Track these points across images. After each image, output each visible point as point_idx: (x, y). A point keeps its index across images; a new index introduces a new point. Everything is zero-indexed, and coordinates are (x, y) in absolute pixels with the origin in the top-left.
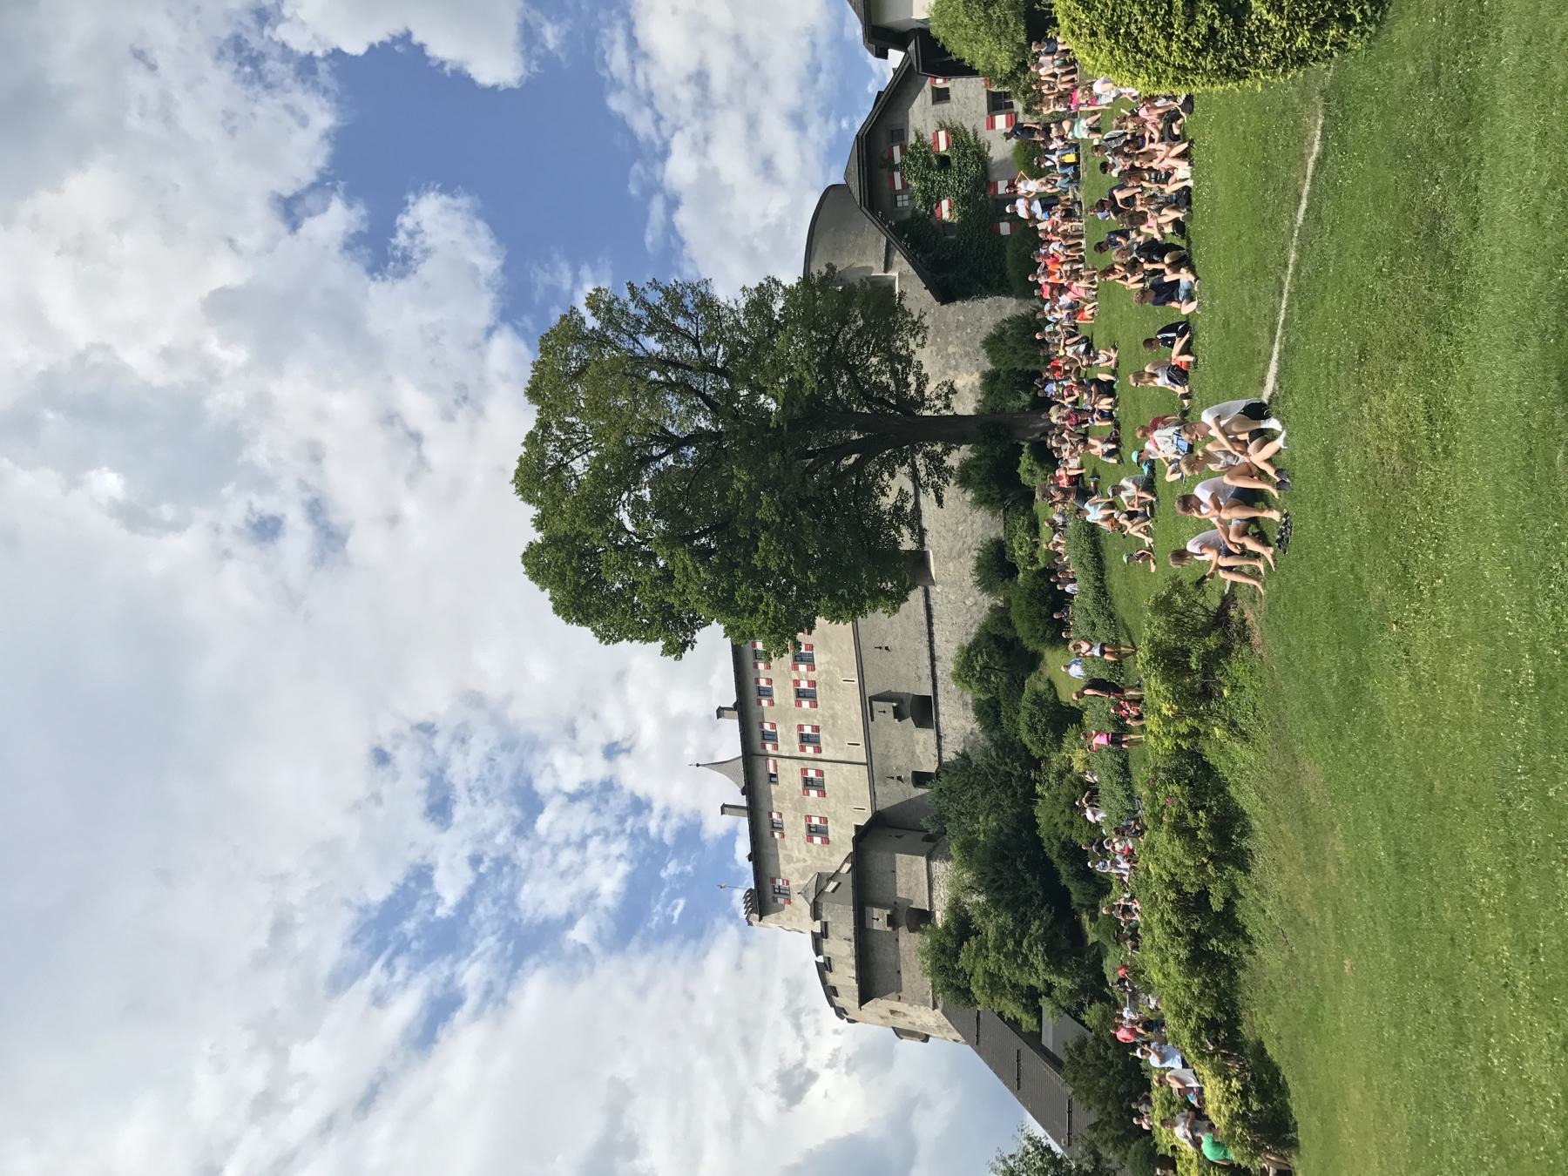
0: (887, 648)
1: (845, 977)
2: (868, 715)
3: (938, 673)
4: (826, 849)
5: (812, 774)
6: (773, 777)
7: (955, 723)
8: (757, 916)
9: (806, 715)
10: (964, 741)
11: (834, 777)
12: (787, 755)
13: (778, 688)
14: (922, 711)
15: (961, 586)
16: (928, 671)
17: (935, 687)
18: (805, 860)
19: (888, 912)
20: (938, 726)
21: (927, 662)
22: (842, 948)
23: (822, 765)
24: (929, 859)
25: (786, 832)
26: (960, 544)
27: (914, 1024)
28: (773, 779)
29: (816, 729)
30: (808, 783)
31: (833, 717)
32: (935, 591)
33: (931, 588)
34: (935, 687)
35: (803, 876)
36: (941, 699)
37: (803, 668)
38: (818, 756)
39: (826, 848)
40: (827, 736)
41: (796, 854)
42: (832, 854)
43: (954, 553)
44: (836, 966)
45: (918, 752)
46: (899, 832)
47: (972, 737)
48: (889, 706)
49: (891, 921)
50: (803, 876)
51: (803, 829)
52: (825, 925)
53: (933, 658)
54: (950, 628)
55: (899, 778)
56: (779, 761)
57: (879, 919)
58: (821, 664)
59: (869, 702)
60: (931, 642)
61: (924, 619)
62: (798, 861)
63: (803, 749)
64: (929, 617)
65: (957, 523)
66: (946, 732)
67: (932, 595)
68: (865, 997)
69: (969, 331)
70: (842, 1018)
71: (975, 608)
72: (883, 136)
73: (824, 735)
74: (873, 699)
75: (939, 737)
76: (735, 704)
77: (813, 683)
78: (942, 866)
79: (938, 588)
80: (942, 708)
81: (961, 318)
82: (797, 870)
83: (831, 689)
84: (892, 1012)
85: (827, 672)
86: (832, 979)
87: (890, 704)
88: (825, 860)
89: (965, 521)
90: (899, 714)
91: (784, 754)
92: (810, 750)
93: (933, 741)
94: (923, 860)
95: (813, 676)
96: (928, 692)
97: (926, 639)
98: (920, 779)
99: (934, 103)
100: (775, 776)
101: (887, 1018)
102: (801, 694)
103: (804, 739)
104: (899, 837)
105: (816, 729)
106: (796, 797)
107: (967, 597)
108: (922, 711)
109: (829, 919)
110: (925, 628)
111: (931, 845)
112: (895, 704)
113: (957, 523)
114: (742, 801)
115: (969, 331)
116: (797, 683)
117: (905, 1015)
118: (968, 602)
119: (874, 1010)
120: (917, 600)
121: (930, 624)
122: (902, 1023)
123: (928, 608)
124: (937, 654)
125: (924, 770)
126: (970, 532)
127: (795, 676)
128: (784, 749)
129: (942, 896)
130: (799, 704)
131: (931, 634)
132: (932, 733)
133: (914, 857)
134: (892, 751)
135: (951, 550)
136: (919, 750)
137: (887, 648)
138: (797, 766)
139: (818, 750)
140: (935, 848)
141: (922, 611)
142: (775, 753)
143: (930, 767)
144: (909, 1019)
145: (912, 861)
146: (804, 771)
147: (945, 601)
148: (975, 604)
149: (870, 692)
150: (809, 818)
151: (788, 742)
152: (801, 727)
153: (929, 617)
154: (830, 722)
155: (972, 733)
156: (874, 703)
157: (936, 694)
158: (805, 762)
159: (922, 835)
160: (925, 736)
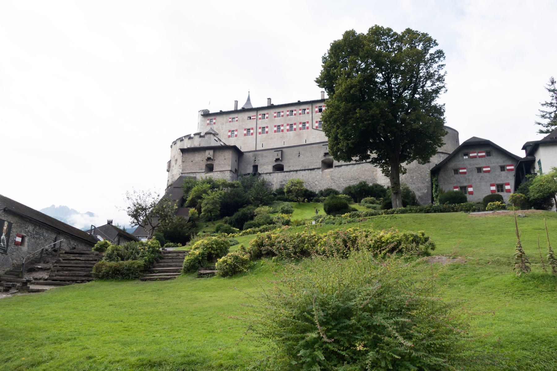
0: (299, 156)
1: (187, 144)
2: (276, 150)
3: (292, 173)
4: (226, 137)
5: (252, 131)
7: (275, 179)
8: (202, 114)
9: (271, 129)
10: (269, 182)
11: (251, 139)
12: (258, 123)
13: (280, 119)
14: (279, 168)
15: (322, 179)
16: (292, 169)
17: (287, 172)
18: (222, 130)
19: (212, 158)
20: (274, 173)
21: (295, 169)
22: (197, 143)
23: (255, 134)
24: (231, 171)
25: (231, 123)
26: (336, 179)
27: (173, 167)
28: (249, 118)
29: (267, 132)
30: (248, 130)
31: (271, 138)
32: (320, 171)
33: (320, 170)
34: (287, 172)
35: (217, 129)
36: (283, 173)
37: (288, 127)
38: (258, 133)
39: (227, 137)
40: (265, 136)
41: (224, 126)
42: (225, 139)
43: (333, 177)
44: (190, 141)
45: (265, 167)
46: (237, 161)
47: (270, 184)
48: (279, 157)
49: (209, 159)
50: (217, 129)
51: (233, 129)
52: (203, 137)
53: (297, 171)
54: (307, 176)
55: (255, 160)
56: (255, 120)
57: (209, 153)
58: (290, 134)
59: (281, 150)
60: (302, 170)
61: (310, 168)
62: (222, 127)
63: (260, 128)
64: (311, 170)
65: (343, 178)
66: (272, 176)
67: (318, 171)
68: (183, 151)
69: (410, 180)
70: (173, 143)
71: (314, 184)
72: (488, 149)
73: (265, 135)
74: (282, 151)
75: (270, 173)
76: (273, 105)
77: (282, 131)
78: (228, 175)
79: (321, 172)
80: (280, 174)
81: (415, 178)
82: (219, 127)
83: (281, 137)
84: (176, 160)
85: (287, 136)
86: (186, 140)
87: (280, 157)
88: (223, 136)
89: (344, 181)
90: (277, 160)
91: (258, 121)
92: (260, 130)
93: (268, 171)
94: (230, 169)
95: (285, 131)
96: (285, 170)
97: (303, 168)
98: (256, 167)
99: (500, 166)
100: (250, 119)
101: (174, 158)
104: (236, 161)
105: (267, 132)
106: (243, 126)
107: (318, 182)
108: (279, 168)
109: (206, 138)
110: (307, 168)
111: (234, 171)
112: (280, 159)
113: (343, 178)
114: (239, 108)
115: (410, 180)
116: (282, 125)
117: (176, 164)
118: (316, 182)
119: (177, 154)
120: (316, 165)
121: (308, 170)
122: (173, 163)
123: (314, 169)
124: (298, 172)
125: (258, 169)
126: (340, 182)
127: (285, 125)
128: (259, 121)
129: (218, 175)
130: (275, 126)
131: (305, 170)
132: (271, 171)
133: (230, 166)
134: (264, 158)
135: (334, 176)
136: (265, 167)
137: (299, 156)
138: (254, 126)
139: (260, 133)
140: (233, 173)
141: (313, 167)
142: (258, 119)
143: (260, 171)
144: (175, 165)
145: (229, 165)
146: (252, 129)
147: (316, 175)
148: (316, 185)
149: (284, 150)
150: (236, 130)
151: (262, 123)
152: (267, 127)
153: (311, 170)
154: (270, 137)
155: (272, 184)
156: (280, 152)
157: (284, 172)
158: (256, 129)
159: (237, 169)
160: (270, 169)
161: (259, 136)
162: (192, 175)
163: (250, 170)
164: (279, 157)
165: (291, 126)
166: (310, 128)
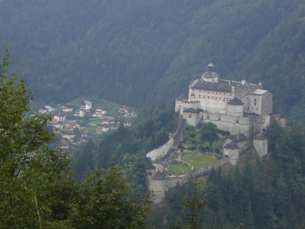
6: (205, 92)
14: (208, 118)
30: (204, 96)
48: (208, 116)
49: (190, 115)
57: (190, 113)
92: (207, 97)
96: (210, 119)
98: (203, 117)
102: (213, 97)
103: (209, 97)
108: (208, 118)
138: (206, 95)
143: (203, 118)
149: (210, 114)
151: (209, 95)
161: (207, 99)
162: (186, 119)
163: (201, 117)
164: (208, 116)
165: (216, 98)
166: (221, 101)
